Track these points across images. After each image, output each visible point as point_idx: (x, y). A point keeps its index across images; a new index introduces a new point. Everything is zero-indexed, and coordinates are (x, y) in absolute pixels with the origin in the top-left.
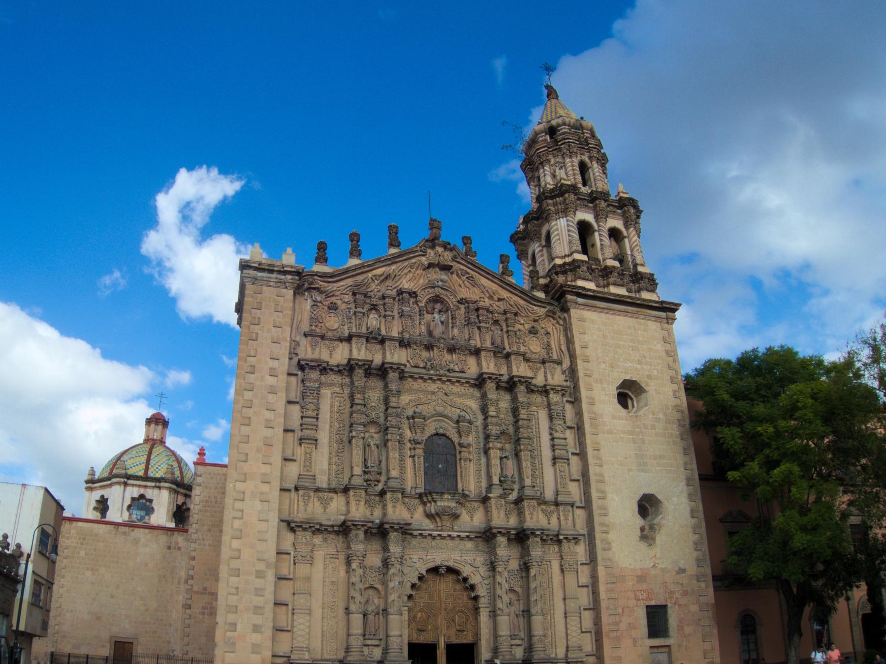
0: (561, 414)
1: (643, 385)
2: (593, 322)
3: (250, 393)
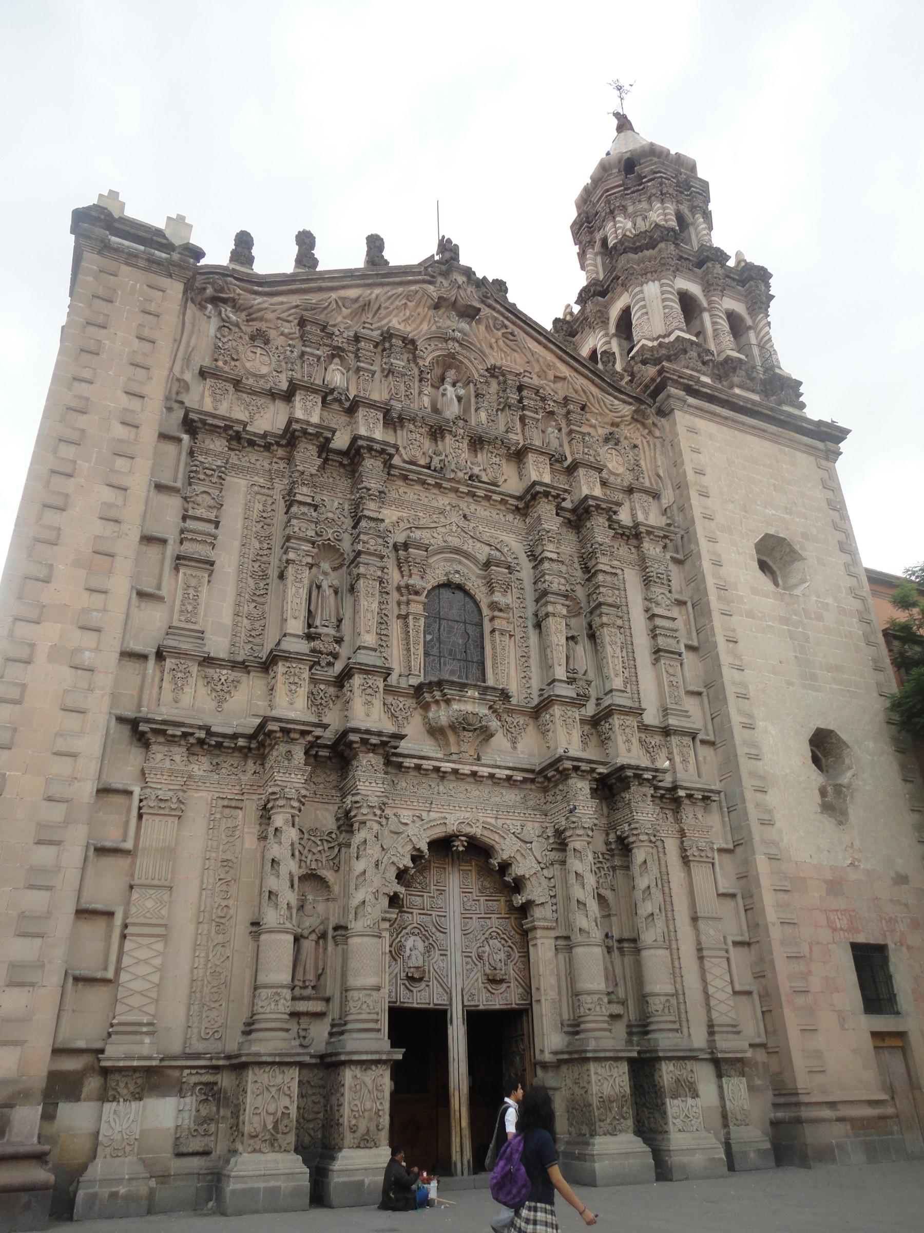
0: (665, 576)
1: (797, 547)
3: (73, 448)
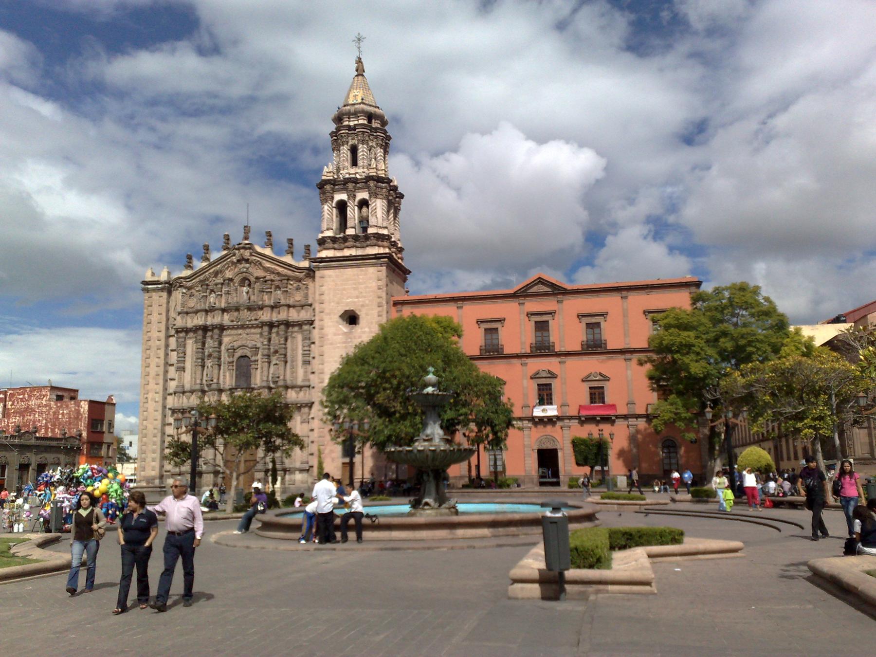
2: (330, 276)
